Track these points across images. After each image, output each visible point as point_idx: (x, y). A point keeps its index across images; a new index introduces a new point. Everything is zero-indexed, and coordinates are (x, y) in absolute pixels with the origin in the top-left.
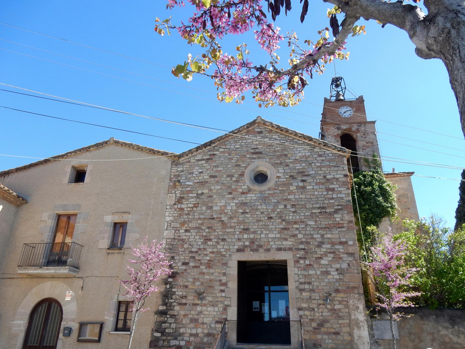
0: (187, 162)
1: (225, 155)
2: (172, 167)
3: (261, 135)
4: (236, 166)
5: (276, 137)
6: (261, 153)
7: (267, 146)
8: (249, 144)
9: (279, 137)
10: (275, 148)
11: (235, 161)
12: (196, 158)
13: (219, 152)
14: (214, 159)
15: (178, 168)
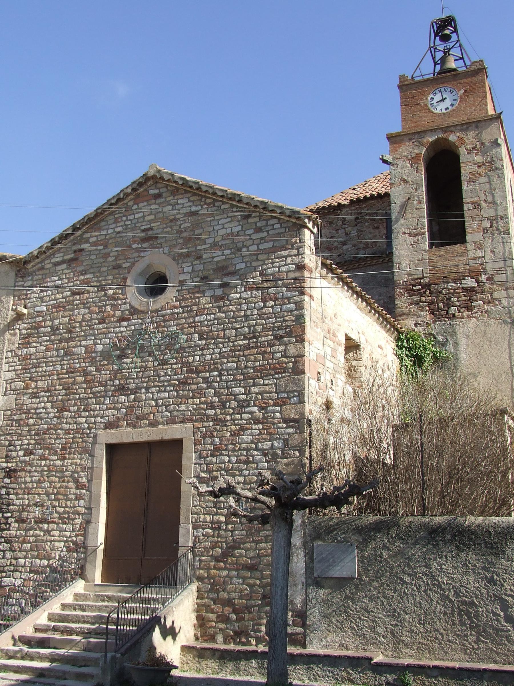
0: (39, 269)
1: (99, 248)
2: (16, 282)
3: (158, 201)
4: (114, 268)
5: (185, 201)
6: (156, 238)
7: (168, 221)
8: (138, 222)
9: (189, 201)
10: (181, 224)
11: (114, 258)
12: (53, 260)
13: (89, 245)
14: (80, 259)
15: (25, 282)
